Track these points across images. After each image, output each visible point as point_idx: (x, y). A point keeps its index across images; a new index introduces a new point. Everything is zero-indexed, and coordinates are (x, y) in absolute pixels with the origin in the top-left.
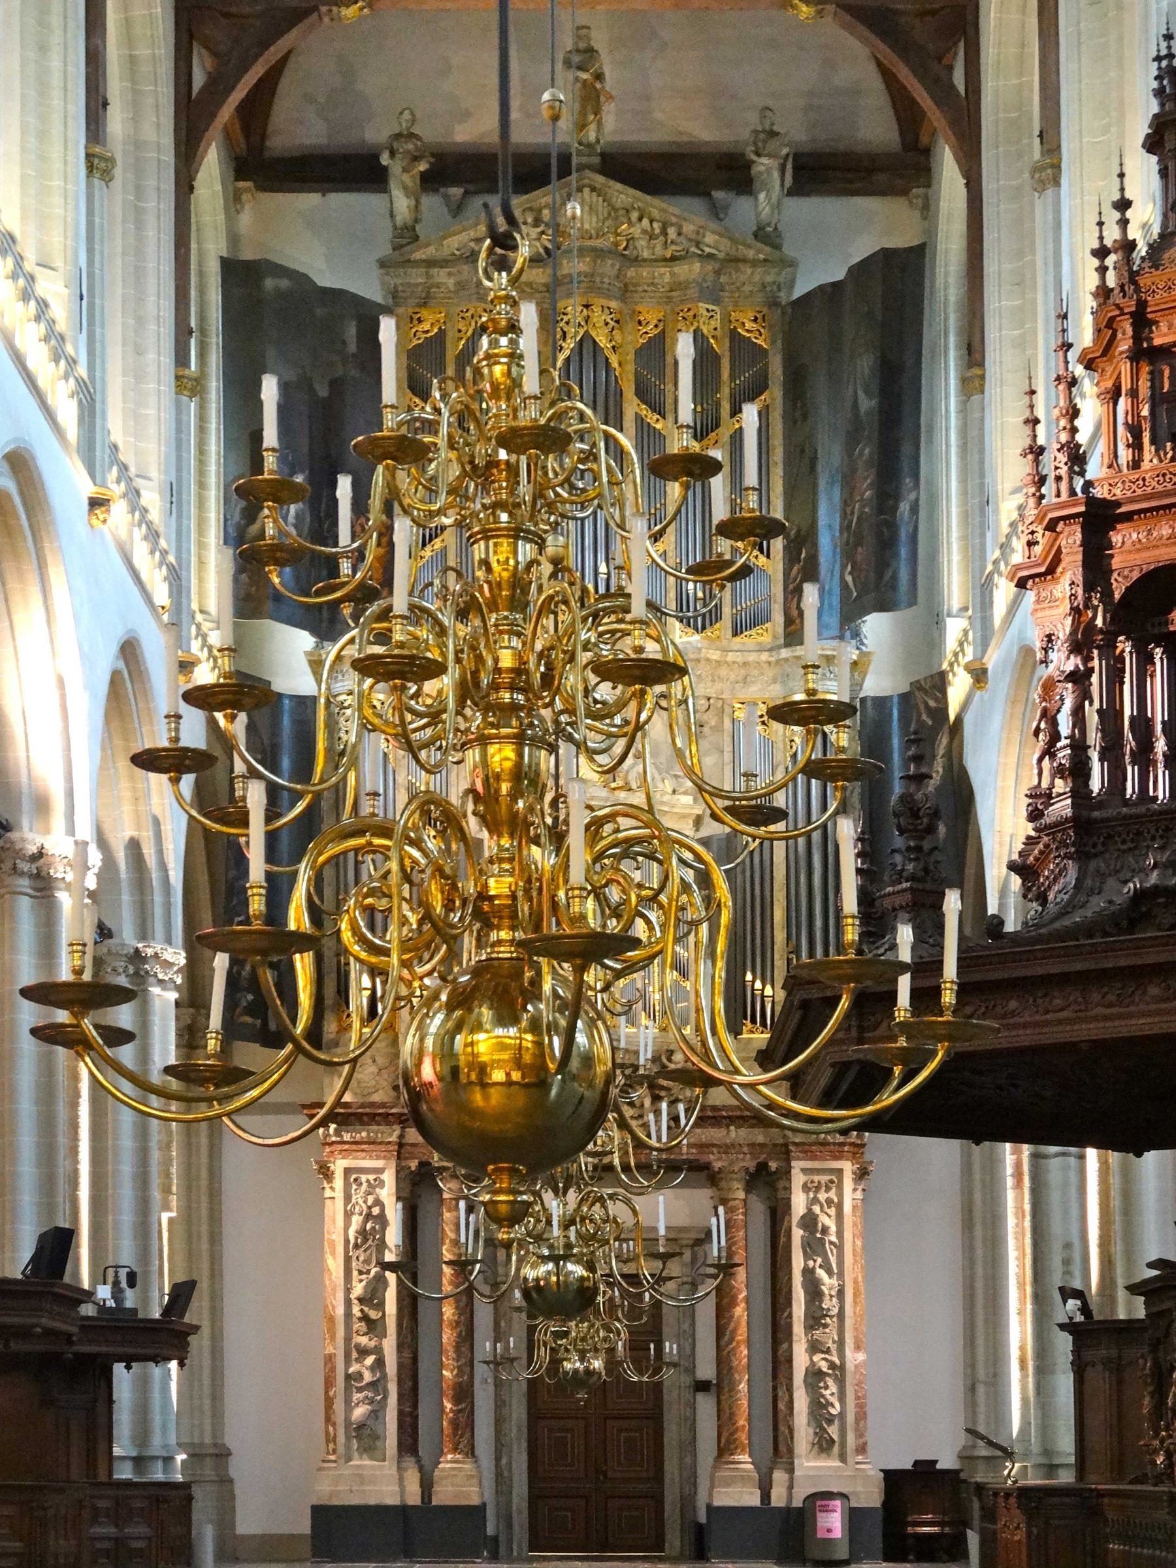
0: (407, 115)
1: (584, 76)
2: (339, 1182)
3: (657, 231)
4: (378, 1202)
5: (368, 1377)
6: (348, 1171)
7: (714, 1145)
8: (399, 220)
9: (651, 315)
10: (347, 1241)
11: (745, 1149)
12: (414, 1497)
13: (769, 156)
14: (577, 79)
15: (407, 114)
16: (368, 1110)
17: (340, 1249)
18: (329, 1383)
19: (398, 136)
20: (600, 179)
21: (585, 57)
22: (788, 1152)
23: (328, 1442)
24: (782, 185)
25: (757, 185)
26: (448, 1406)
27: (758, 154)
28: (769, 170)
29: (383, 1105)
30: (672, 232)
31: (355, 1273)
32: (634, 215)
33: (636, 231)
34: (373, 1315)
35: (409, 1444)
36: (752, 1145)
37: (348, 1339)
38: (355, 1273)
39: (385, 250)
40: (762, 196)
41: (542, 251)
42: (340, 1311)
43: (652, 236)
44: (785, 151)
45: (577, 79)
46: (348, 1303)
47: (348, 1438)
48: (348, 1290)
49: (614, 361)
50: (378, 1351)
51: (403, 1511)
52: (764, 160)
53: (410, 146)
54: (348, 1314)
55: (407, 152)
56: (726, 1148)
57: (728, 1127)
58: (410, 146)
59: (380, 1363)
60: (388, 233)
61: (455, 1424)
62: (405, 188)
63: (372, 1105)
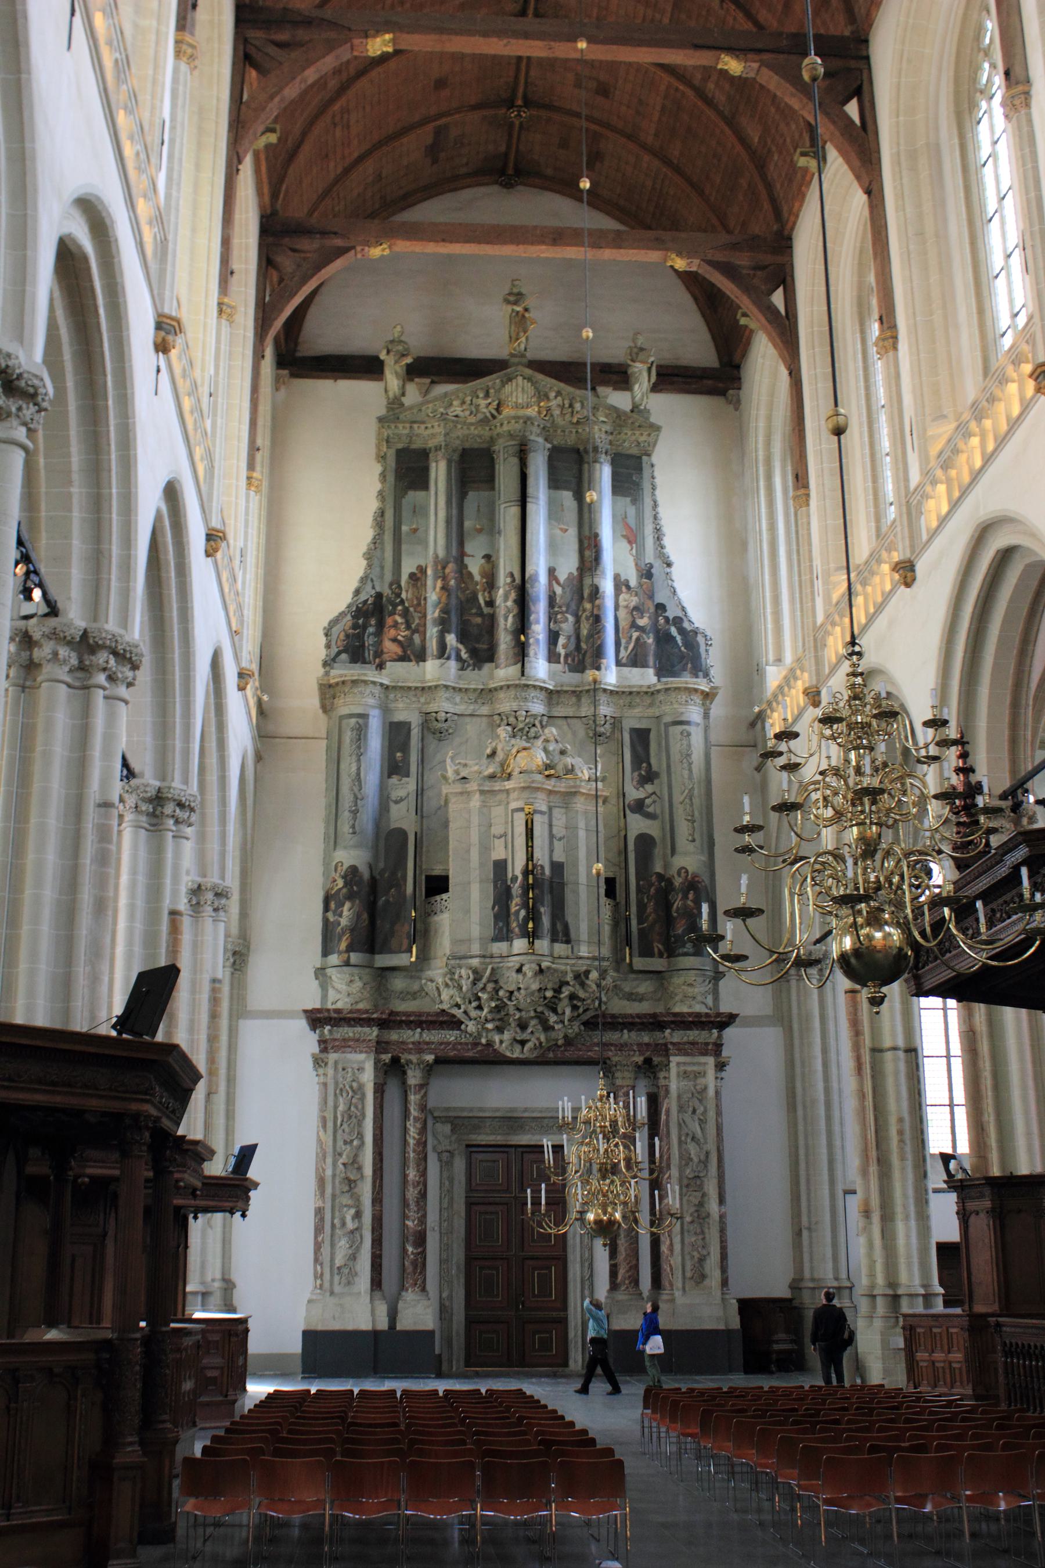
0: (399, 328)
1: (518, 309)
2: (330, 1071)
3: (567, 406)
5: (350, 1225)
6: (336, 1063)
7: (612, 1045)
8: (391, 394)
10: (335, 1118)
11: (635, 1048)
12: (383, 1324)
13: (642, 362)
14: (513, 310)
15: (399, 328)
16: (355, 1015)
17: (330, 1125)
18: (319, 1229)
19: (392, 342)
20: (528, 372)
21: (516, 297)
22: (667, 1050)
23: (316, 1278)
24: (649, 380)
25: (632, 379)
26: (410, 1249)
27: (633, 361)
28: (640, 371)
29: (367, 1012)
30: (578, 406)
32: (552, 395)
33: (553, 403)
35: (376, 1283)
36: (639, 1045)
37: (334, 1196)
38: (340, 1143)
39: (382, 411)
40: (636, 387)
41: (488, 415)
42: (329, 1172)
43: (562, 407)
44: (652, 359)
45: (513, 310)
47: (332, 1275)
51: (375, 1334)
52: (638, 365)
53: (400, 348)
54: (334, 1176)
55: (398, 351)
56: (621, 1047)
57: (622, 1030)
58: (400, 348)
59: (358, 1215)
60: (385, 402)
61: (414, 1263)
62: (396, 373)
63: (358, 1011)
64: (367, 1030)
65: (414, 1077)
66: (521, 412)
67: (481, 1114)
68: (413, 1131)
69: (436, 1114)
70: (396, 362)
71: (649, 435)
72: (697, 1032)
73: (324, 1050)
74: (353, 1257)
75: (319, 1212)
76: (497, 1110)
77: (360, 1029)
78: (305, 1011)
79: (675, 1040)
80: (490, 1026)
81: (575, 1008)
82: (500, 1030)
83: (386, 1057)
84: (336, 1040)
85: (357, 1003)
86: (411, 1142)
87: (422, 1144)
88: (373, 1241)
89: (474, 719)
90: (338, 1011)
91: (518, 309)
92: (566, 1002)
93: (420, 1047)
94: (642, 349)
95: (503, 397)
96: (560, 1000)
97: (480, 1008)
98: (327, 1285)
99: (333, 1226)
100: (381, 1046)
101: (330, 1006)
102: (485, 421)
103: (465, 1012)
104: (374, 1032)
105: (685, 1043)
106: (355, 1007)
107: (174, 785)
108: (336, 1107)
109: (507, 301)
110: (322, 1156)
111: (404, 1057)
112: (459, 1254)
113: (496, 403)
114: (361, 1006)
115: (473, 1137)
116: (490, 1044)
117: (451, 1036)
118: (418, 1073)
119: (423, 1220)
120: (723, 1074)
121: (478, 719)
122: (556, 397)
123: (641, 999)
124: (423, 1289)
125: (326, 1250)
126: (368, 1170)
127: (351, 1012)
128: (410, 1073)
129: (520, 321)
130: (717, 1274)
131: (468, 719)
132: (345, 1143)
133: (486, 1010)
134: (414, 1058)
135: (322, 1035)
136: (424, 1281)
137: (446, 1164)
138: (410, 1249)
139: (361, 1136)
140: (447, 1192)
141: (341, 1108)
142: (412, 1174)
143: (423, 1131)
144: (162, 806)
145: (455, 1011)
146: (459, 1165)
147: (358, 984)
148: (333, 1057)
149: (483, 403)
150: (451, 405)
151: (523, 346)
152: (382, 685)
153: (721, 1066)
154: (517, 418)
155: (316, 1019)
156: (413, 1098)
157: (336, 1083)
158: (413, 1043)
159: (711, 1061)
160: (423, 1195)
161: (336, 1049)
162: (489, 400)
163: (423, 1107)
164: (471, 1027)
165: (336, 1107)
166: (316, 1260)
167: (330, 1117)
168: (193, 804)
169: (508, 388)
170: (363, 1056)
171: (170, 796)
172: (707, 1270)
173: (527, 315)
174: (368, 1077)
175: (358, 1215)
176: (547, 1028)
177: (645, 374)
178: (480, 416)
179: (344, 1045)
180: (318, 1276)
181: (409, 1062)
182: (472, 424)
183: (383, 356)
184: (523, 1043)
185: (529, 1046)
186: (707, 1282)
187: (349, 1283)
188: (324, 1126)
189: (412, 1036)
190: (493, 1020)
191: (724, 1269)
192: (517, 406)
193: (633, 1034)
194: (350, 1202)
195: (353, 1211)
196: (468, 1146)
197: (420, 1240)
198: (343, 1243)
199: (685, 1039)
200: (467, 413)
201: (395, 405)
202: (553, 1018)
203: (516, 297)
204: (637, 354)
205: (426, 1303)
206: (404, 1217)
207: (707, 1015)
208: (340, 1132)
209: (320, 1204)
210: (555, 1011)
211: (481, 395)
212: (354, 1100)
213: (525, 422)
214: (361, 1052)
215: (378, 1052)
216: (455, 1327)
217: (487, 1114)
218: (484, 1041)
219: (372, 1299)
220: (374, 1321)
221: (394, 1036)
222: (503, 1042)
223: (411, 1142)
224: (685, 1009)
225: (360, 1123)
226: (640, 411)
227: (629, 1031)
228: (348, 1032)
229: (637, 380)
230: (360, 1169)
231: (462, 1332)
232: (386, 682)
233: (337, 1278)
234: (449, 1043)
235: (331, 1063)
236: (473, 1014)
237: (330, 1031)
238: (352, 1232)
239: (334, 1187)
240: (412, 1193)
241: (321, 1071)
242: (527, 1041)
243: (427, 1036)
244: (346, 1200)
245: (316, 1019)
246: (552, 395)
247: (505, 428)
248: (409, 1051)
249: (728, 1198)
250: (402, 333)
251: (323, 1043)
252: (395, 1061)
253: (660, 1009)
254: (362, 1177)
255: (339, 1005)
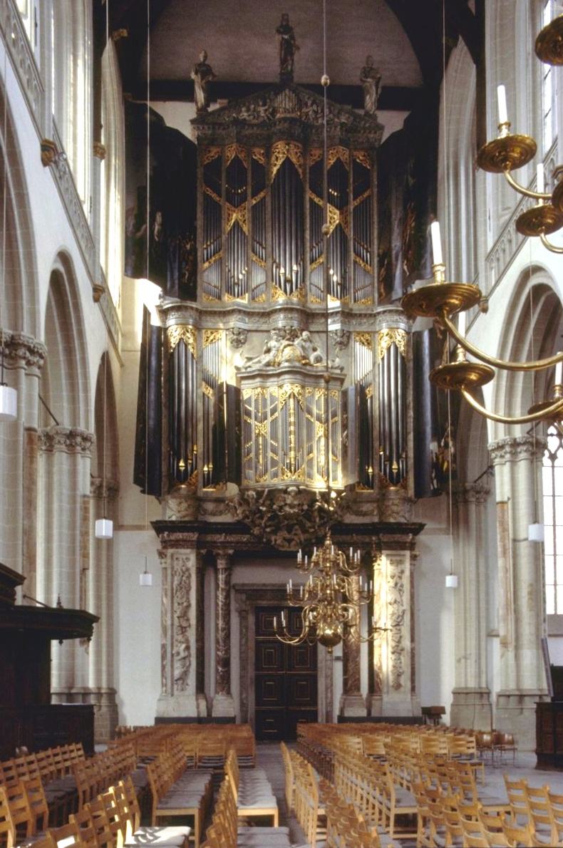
1: (286, 37)
2: (169, 561)
4: (188, 570)
5: (182, 655)
6: (172, 556)
9: (317, 152)
10: (172, 589)
14: (283, 38)
17: (169, 593)
18: (163, 657)
21: (285, 28)
24: (377, 93)
31: (176, 605)
32: (309, 103)
34: (184, 624)
35: (201, 688)
36: (363, 543)
37: (172, 637)
38: (176, 605)
42: (169, 622)
43: (316, 112)
45: (283, 38)
46: (172, 617)
47: (172, 685)
48: (173, 612)
49: (300, 171)
50: (187, 641)
54: (172, 625)
59: (188, 648)
63: (185, 522)
64: (191, 534)
65: (221, 564)
66: (288, 115)
67: (264, 588)
68: (221, 597)
69: (237, 588)
70: (202, 79)
71: (375, 133)
72: (399, 536)
73: (164, 547)
74: (185, 673)
75: (163, 646)
76: (273, 585)
77: (186, 534)
78: (152, 523)
79: (385, 540)
80: (268, 530)
81: (322, 518)
82: (274, 532)
83: (203, 551)
84: (171, 541)
85: (184, 517)
86: (220, 604)
87: (227, 605)
88: (197, 664)
89: (258, 334)
90: (172, 522)
91: (286, 37)
92: (316, 514)
93: (225, 545)
94: (371, 69)
95: (276, 105)
96: (312, 512)
97: (262, 518)
98: (169, 690)
99: (172, 655)
100: (198, 545)
101: (167, 519)
102: (262, 125)
103: (252, 521)
104: (194, 536)
105: (391, 542)
106: (183, 519)
107: (22, 333)
108: (172, 583)
109: (278, 32)
110: (164, 614)
111: (215, 551)
112: (251, 672)
113: (271, 110)
114: (186, 519)
115: (260, 602)
116: (269, 541)
117: (245, 538)
118: (224, 562)
119: (228, 651)
120: (415, 562)
121: (261, 334)
122: (312, 105)
123: (364, 514)
124: (229, 693)
125: (168, 668)
126: (193, 621)
127: (181, 522)
128: (219, 561)
129: (288, 49)
130: (409, 684)
131: (254, 334)
132: (179, 604)
133: (265, 519)
134: (221, 552)
135: (163, 537)
136: (229, 688)
137: (243, 615)
138: (220, 669)
139: (188, 600)
140: (243, 635)
141: (176, 583)
142: (221, 623)
143: (227, 597)
144: (16, 350)
145: (247, 521)
146: (251, 619)
147: (184, 505)
148: (170, 551)
149: (262, 109)
150: (241, 111)
151: (289, 67)
152: (197, 310)
153: (414, 558)
154: (285, 119)
155: (159, 527)
156: (221, 577)
157: (173, 568)
158: (221, 543)
159: (408, 553)
160: (228, 637)
161: (172, 546)
162: (266, 107)
163: (227, 582)
164: (256, 531)
165: (172, 583)
166: (163, 676)
167: (169, 587)
168: (40, 351)
169: (280, 98)
170: (188, 551)
171: (21, 342)
172: (402, 682)
173: (292, 42)
174: (192, 563)
175: (188, 648)
176: (305, 531)
177: (374, 88)
178: (261, 119)
179: (176, 544)
180: (164, 685)
181: (218, 554)
182: (255, 125)
183: (193, 76)
184: (289, 541)
185: (293, 543)
186: (402, 689)
187: (182, 690)
188: (166, 595)
189: (221, 538)
190: (270, 526)
191: (413, 681)
192: (286, 110)
193: (359, 537)
194: (183, 640)
195: (184, 646)
196: (256, 607)
197: (225, 663)
198: (177, 665)
199: (392, 540)
200: (252, 117)
201: (202, 111)
202: (308, 524)
203: (285, 28)
204: (369, 72)
205: (231, 701)
206: (218, 649)
207: (406, 524)
208: (175, 597)
209: (164, 642)
210: (310, 521)
211: (261, 103)
212: (184, 578)
213: (290, 123)
214: (188, 548)
215: (198, 548)
216: (249, 716)
217: (268, 588)
218: (265, 540)
219: (197, 699)
220: (199, 712)
221: (209, 538)
222: (278, 539)
223: (220, 604)
224: (392, 520)
225: (188, 592)
226: (370, 115)
227: (357, 535)
228: (180, 536)
229: (368, 92)
230: (188, 620)
231: (253, 716)
232: (199, 307)
233: (175, 686)
234: (243, 543)
235: (169, 555)
236: (258, 522)
237: (168, 536)
238: (184, 658)
239: (172, 632)
240: (221, 635)
241: (163, 561)
242: (293, 540)
243: (230, 538)
244: (180, 638)
245: (159, 527)
246: (309, 103)
247: (278, 127)
248: (218, 548)
249: (416, 638)
250: (206, 57)
251: (166, 544)
252: (209, 553)
253: (376, 520)
254: (190, 626)
255: (174, 518)
